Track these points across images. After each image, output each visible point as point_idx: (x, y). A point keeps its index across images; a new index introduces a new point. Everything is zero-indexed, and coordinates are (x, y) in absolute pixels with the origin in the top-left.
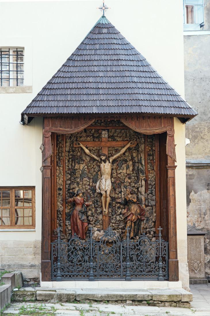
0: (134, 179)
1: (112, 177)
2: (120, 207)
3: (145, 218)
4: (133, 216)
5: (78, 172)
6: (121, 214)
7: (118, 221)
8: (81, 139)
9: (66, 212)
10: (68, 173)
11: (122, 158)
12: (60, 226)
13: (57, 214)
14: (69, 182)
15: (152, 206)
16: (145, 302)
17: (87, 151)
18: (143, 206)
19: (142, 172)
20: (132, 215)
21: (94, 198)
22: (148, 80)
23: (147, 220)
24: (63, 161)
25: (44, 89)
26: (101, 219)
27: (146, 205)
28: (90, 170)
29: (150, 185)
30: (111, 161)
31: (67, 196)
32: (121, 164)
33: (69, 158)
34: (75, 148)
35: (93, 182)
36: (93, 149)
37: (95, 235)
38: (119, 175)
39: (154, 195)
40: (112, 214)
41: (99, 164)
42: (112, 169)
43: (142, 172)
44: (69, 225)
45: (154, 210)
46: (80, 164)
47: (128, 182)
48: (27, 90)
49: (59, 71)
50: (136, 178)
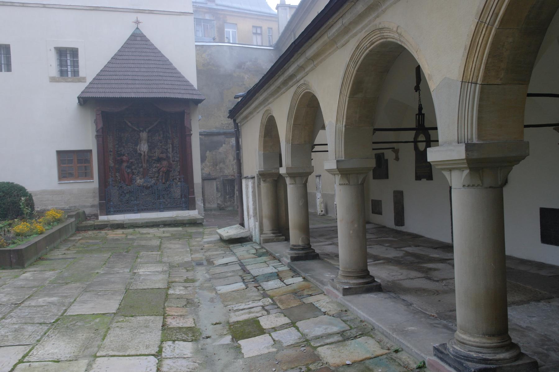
1: (148, 142)
6: (155, 167)
12: (112, 177)
14: (117, 146)
15: (176, 161)
16: (173, 225)
17: (129, 124)
18: (171, 161)
20: (163, 168)
22: (171, 75)
25: (94, 79)
30: (147, 131)
37: (138, 181)
42: (148, 137)
48: (83, 80)
49: (105, 66)
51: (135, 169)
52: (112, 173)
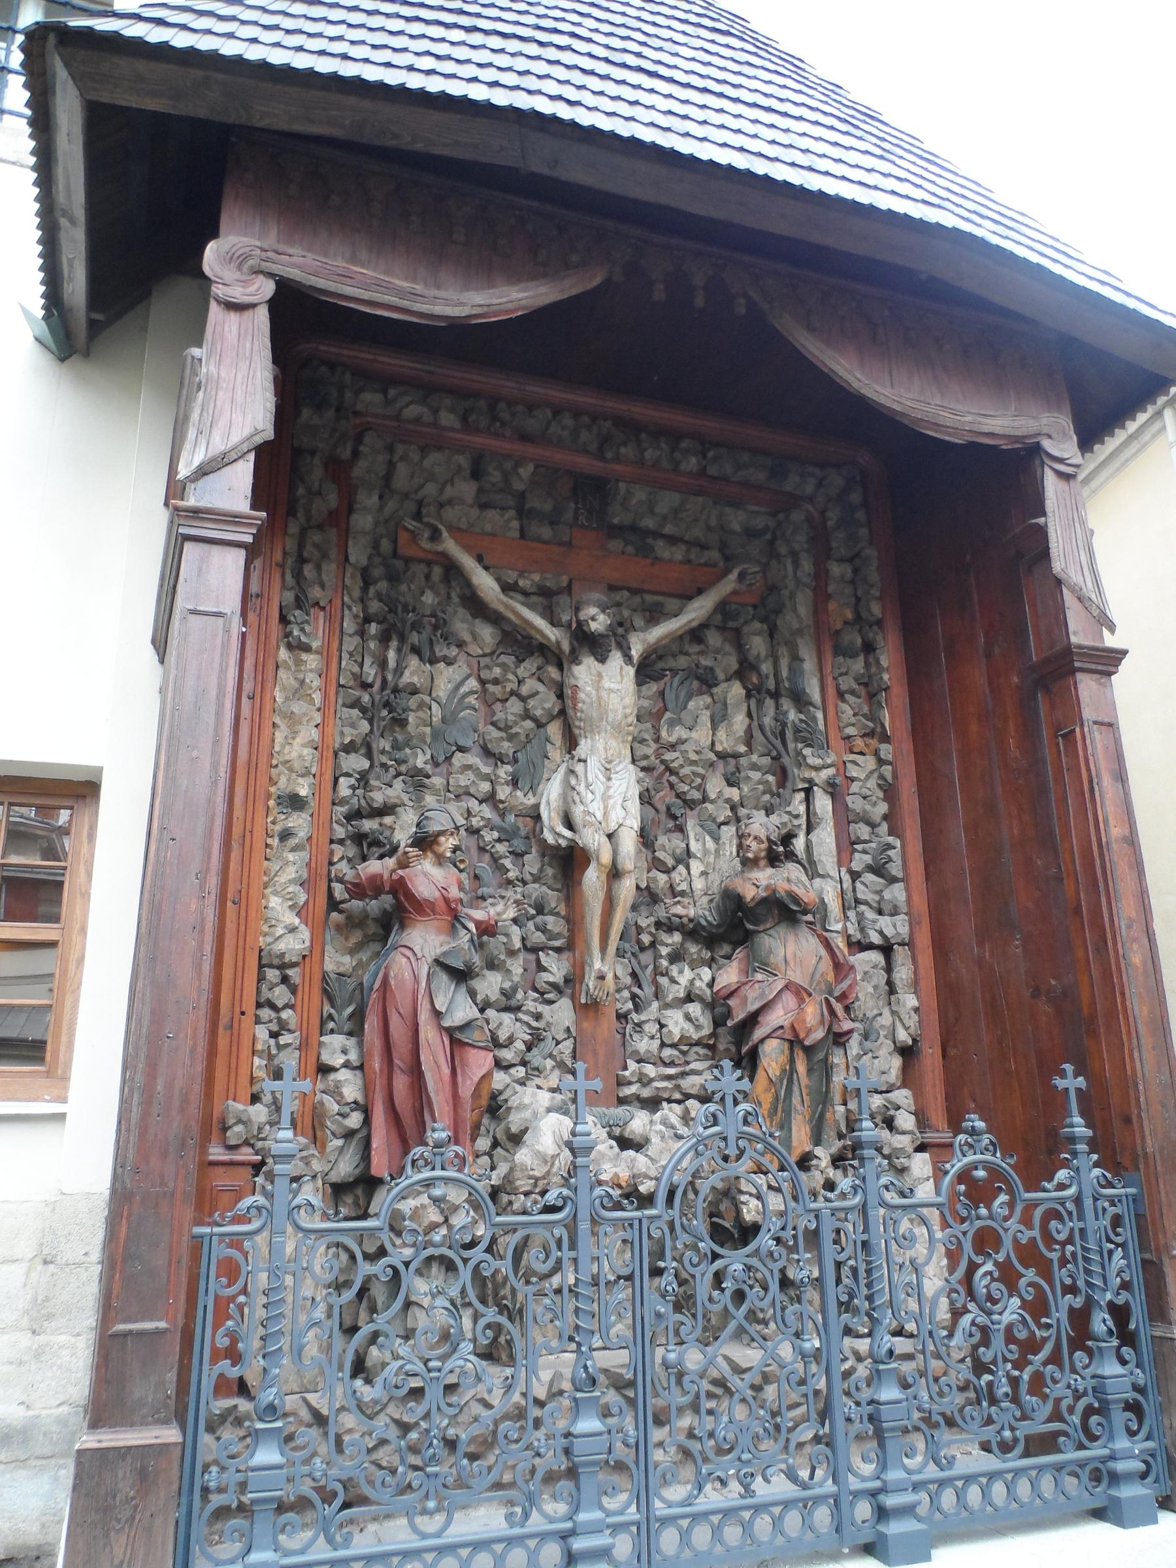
0: (761, 787)
2: (686, 951)
3: (857, 1025)
4: (801, 1001)
6: (689, 998)
7: (673, 1046)
8: (450, 514)
9: (329, 967)
13: (261, 978)
14: (356, 762)
21: (519, 890)
23: (866, 1036)
27: (849, 936)
30: (636, 652)
32: (682, 695)
33: (367, 620)
34: (408, 561)
35: (514, 783)
36: (521, 583)
38: (669, 756)
39: (893, 880)
44: (347, 1065)
45: (903, 973)
47: (728, 801)
50: (771, 778)
52: (283, 1027)
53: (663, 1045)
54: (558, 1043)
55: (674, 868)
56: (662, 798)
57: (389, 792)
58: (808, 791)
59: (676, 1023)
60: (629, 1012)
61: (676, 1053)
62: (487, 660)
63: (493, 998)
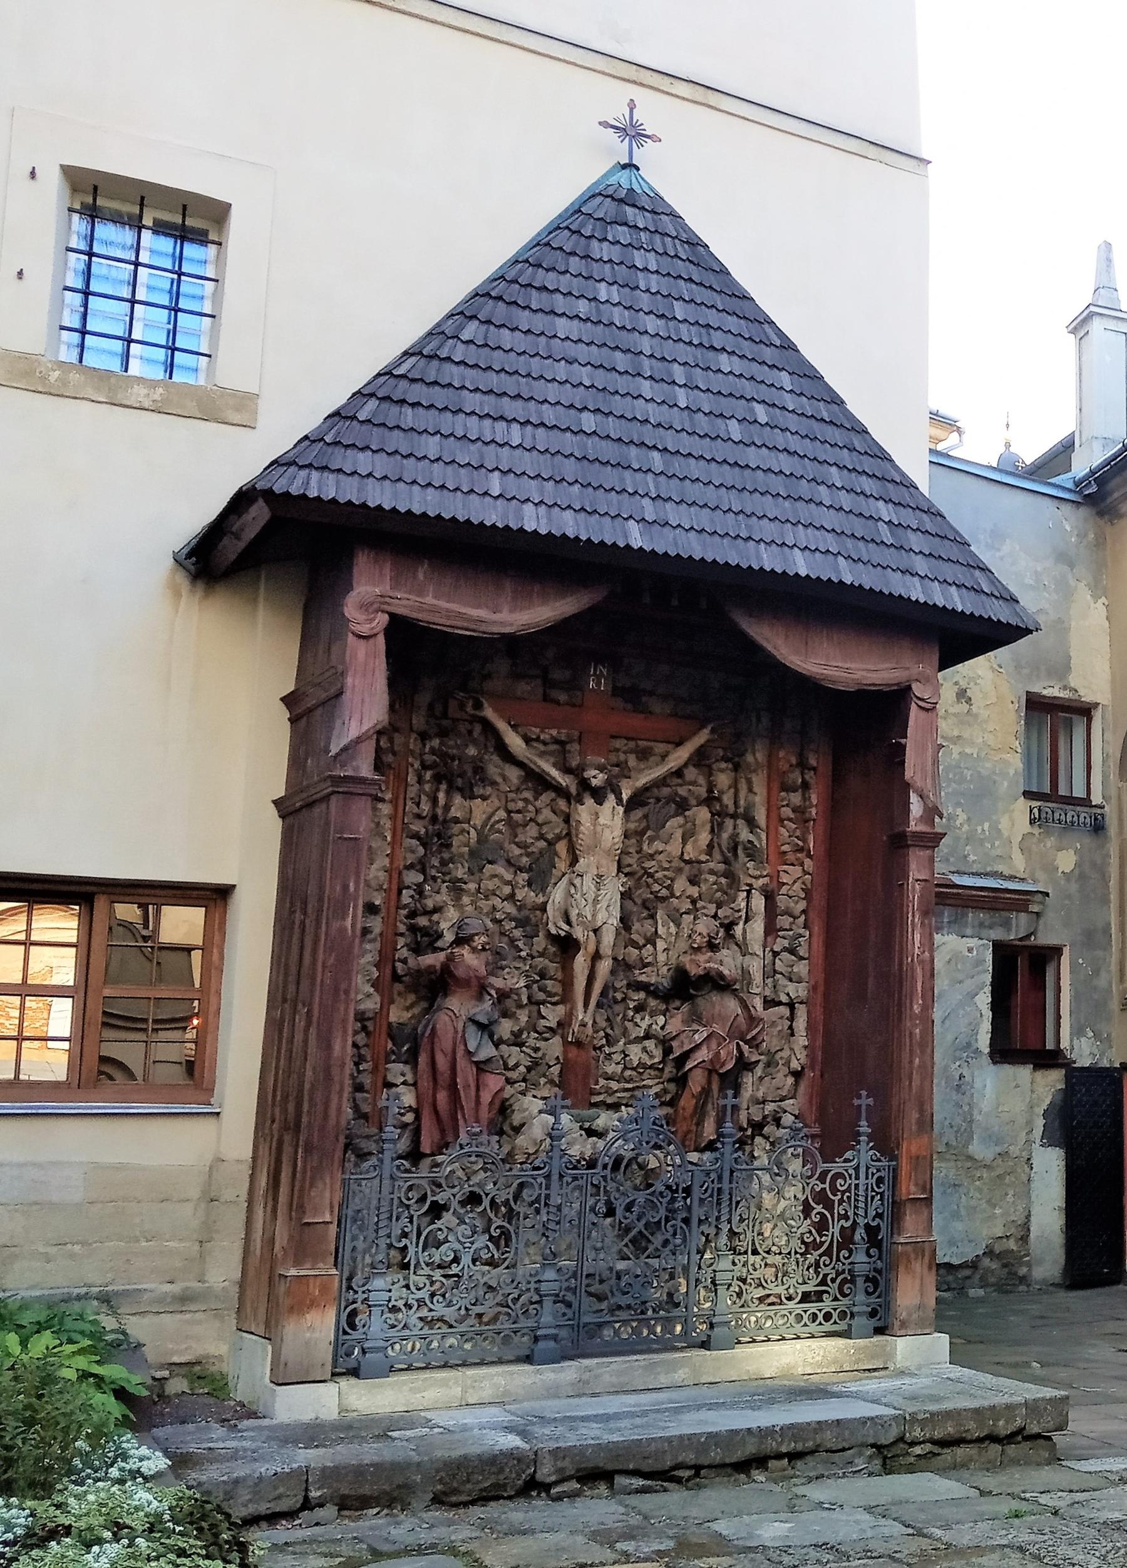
5: (463, 831)
6: (647, 1036)
8: (489, 685)
10: (416, 836)
11: (666, 791)
14: (413, 877)
19: (752, 852)
24: (397, 777)
26: (558, 1058)
28: (520, 830)
29: (788, 913)
31: (401, 941)
38: (647, 865)
39: (802, 958)
40: (607, 1036)
41: (562, 804)
43: (752, 852)
46: (472, 797)
47: (688, 897)
50: (723, 880)
51: (517, 1041)
53: (625, 1068)
54: (550, 1067)
55: (645, 946)
56: (640, 895)
57: (438, 898)
58: (749, 892)
59: (635, 1054)
60: (603, 1046)
61: (634, 1073)
62: (511, 795)
63: (505, 1038)
